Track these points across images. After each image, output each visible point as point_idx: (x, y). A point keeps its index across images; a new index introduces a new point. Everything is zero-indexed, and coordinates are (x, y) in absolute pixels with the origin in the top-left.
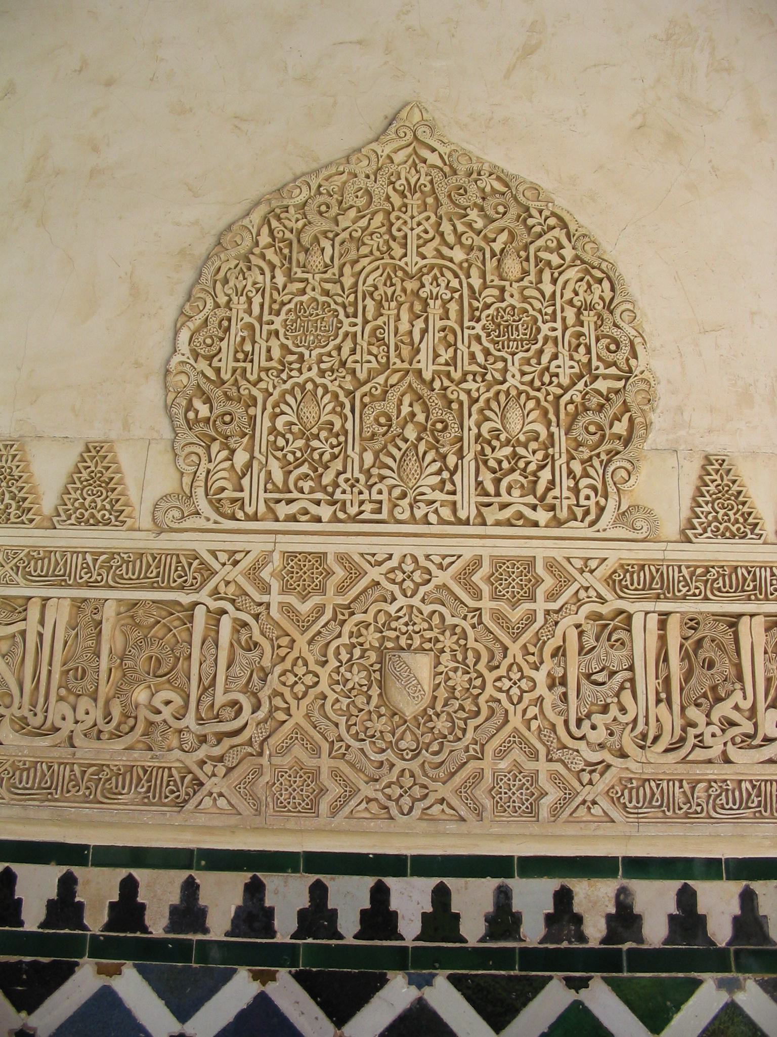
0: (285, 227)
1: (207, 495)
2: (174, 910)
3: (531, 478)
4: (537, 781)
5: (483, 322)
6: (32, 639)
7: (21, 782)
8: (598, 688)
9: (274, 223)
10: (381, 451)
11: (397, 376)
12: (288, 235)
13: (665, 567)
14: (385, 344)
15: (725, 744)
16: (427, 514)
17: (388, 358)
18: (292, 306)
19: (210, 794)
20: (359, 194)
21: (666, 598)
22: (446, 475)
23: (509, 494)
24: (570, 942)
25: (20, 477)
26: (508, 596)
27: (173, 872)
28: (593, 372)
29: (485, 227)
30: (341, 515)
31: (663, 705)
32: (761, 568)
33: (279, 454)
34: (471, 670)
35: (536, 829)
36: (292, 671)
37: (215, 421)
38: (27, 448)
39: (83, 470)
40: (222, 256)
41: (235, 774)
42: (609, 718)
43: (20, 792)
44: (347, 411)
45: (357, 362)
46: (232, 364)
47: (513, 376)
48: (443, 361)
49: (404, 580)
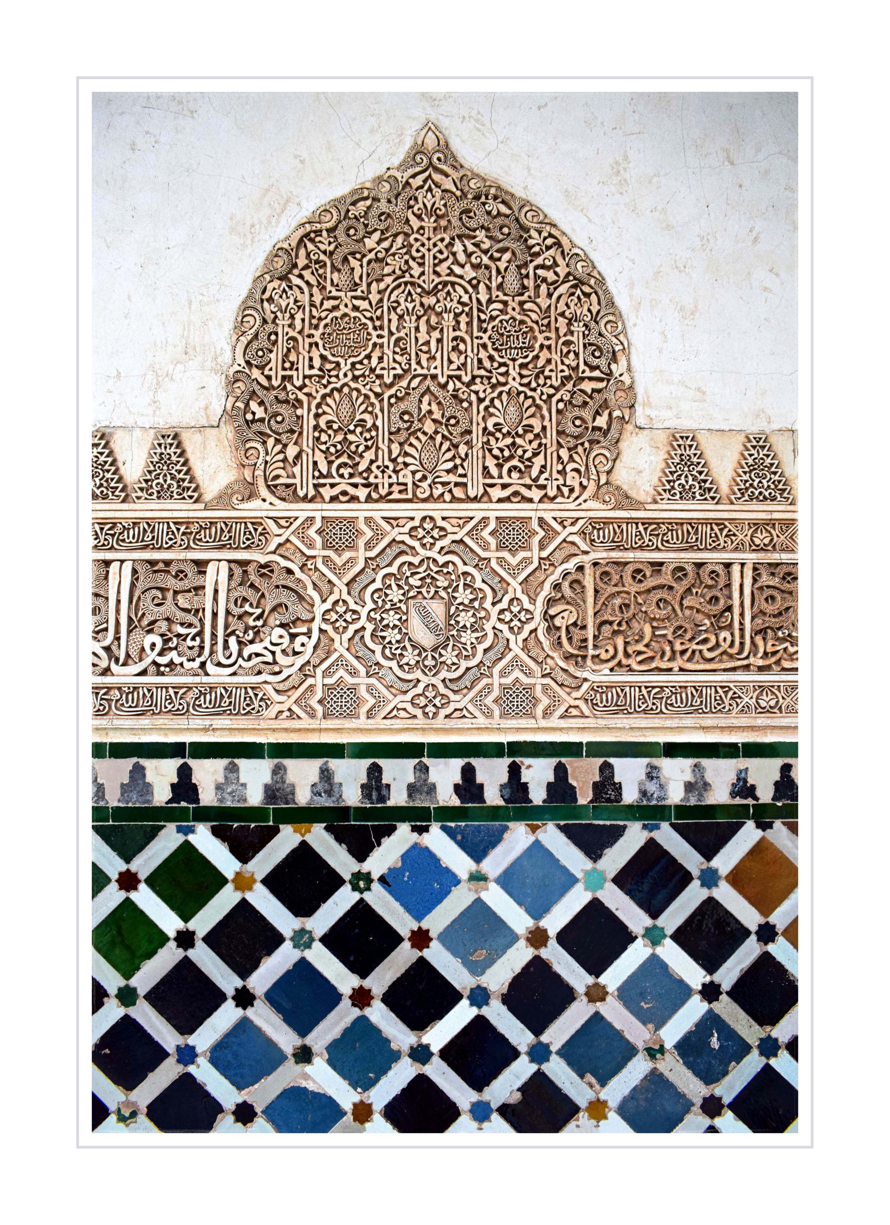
0: (319, 249)
1: (266, 480)
3: (527, 463)
5: (489, 332)
9: (310, 246)
10: (405, 442)
12: (323, 257)
14: (406, 353)
16: (442, 494)
17: (410, 365)
18: (328, 320)
20: (383, 218)
22: (458, 461)
23: (510, 477)
28: (580, 375)
33: (323, 447)
37: (269, 421)
44: (377, 410)
45: (383, 369)
47: (514, 379)
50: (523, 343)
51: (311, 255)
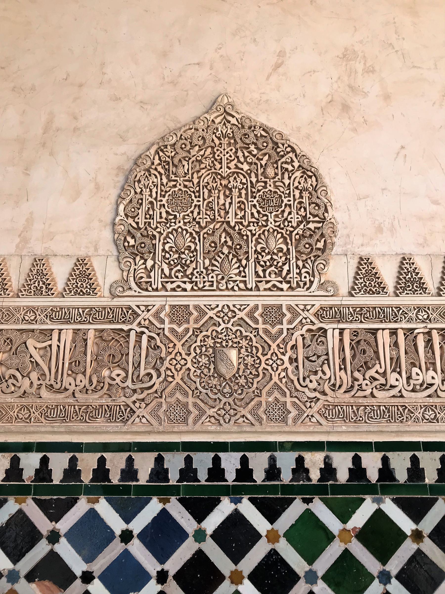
0: (165, 155)
1: (135, 280)
2: (123, 471)
3: (279, 269)
4: (286, 406)
5: (257, 198)
6: (54, 348)
7: (50, 415)
8: (312, 363)
9: (161, 154)
10: (213, 258)
11: (220, 224)
12: (167, 159)
13: (342, 308)
14: (213, 210)
15: (372, 389)
16: (233, 287)
17: (215, 216)
18: (170, 193)
19: (138, 416)
20: (200, 139)
21: (343, 322)
22: (241, 269)
24: (304, 481)
25: (47, 274)
26: (270, 322)
27: (122, 454)
29: (258, 153)
30: (195, 288)
31: (343, 371)
32: (387, 307)
33: (167, 261)
34: (255, 356)
35: (287, 429)
36: (175, 359)
38: (50, 261)
39: (76, 270)
40: (138, 170)
41: (150, 406)
42: (318, 377)
43: (50, 419)
44: (197, 241)
45: (200, 218)
46: (144, 220)
47: (271, 223)
48: (240, 217)
49: (224, 316)
50: (276, 203)
51: (162, 158)
